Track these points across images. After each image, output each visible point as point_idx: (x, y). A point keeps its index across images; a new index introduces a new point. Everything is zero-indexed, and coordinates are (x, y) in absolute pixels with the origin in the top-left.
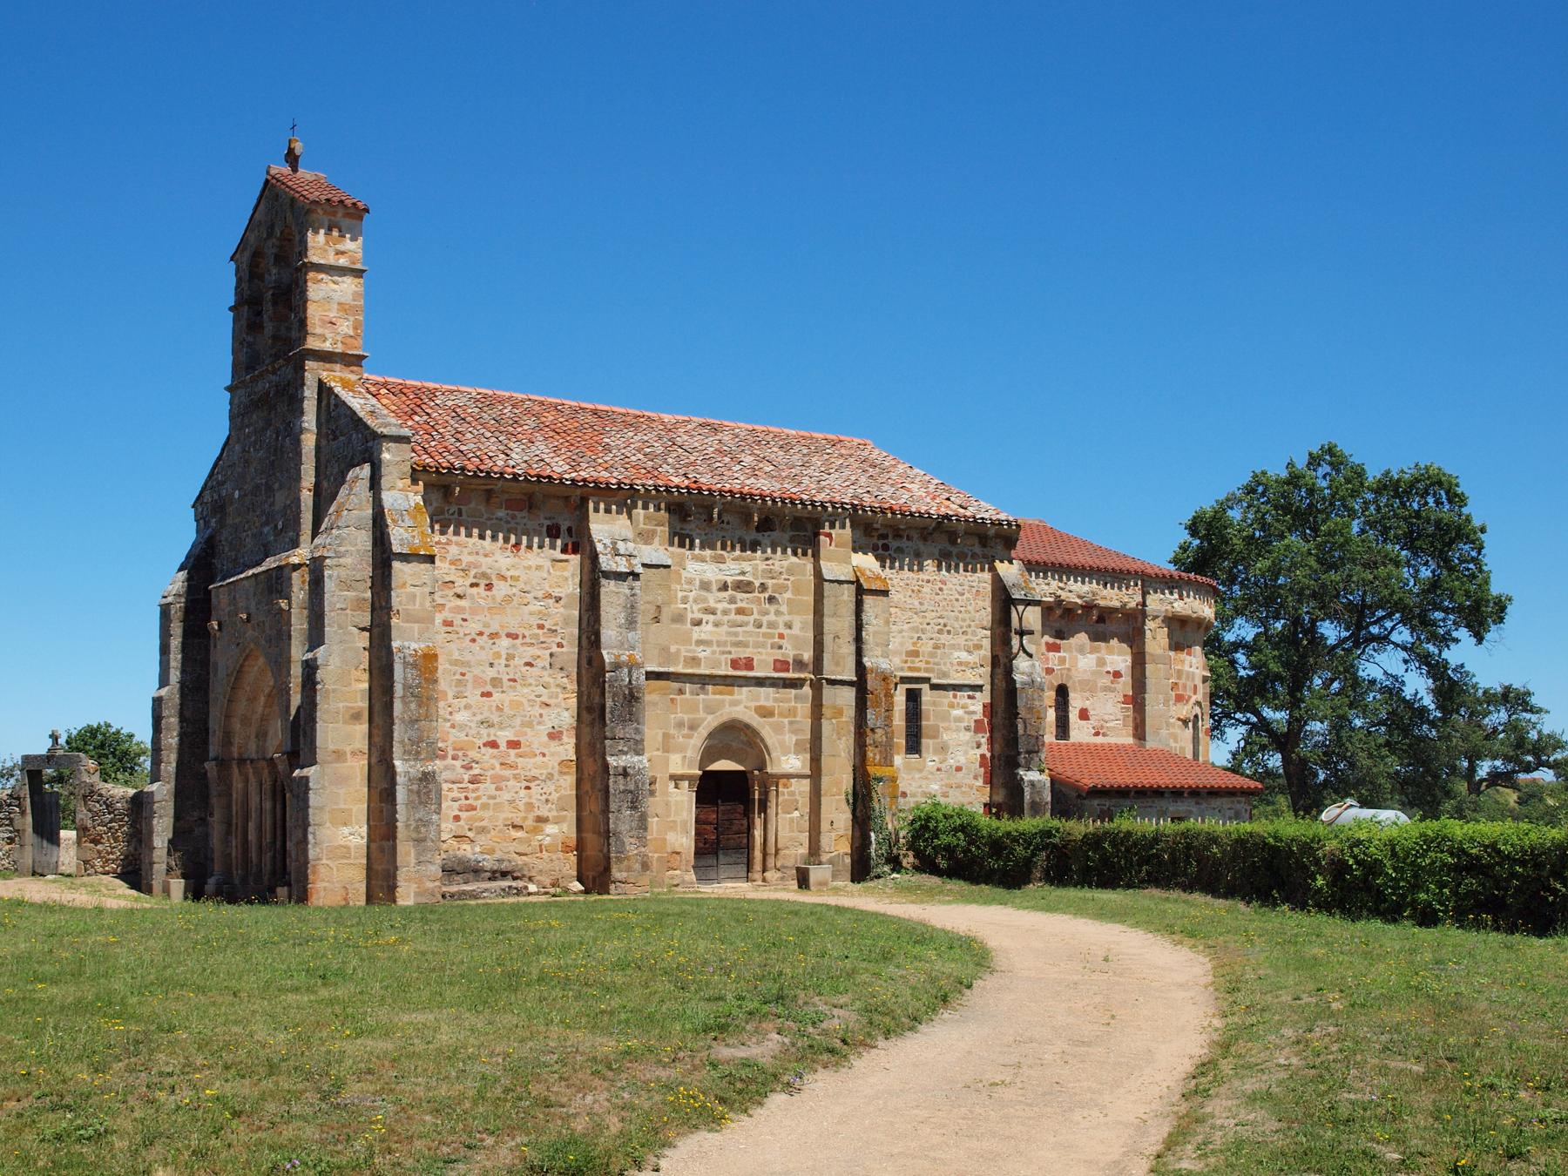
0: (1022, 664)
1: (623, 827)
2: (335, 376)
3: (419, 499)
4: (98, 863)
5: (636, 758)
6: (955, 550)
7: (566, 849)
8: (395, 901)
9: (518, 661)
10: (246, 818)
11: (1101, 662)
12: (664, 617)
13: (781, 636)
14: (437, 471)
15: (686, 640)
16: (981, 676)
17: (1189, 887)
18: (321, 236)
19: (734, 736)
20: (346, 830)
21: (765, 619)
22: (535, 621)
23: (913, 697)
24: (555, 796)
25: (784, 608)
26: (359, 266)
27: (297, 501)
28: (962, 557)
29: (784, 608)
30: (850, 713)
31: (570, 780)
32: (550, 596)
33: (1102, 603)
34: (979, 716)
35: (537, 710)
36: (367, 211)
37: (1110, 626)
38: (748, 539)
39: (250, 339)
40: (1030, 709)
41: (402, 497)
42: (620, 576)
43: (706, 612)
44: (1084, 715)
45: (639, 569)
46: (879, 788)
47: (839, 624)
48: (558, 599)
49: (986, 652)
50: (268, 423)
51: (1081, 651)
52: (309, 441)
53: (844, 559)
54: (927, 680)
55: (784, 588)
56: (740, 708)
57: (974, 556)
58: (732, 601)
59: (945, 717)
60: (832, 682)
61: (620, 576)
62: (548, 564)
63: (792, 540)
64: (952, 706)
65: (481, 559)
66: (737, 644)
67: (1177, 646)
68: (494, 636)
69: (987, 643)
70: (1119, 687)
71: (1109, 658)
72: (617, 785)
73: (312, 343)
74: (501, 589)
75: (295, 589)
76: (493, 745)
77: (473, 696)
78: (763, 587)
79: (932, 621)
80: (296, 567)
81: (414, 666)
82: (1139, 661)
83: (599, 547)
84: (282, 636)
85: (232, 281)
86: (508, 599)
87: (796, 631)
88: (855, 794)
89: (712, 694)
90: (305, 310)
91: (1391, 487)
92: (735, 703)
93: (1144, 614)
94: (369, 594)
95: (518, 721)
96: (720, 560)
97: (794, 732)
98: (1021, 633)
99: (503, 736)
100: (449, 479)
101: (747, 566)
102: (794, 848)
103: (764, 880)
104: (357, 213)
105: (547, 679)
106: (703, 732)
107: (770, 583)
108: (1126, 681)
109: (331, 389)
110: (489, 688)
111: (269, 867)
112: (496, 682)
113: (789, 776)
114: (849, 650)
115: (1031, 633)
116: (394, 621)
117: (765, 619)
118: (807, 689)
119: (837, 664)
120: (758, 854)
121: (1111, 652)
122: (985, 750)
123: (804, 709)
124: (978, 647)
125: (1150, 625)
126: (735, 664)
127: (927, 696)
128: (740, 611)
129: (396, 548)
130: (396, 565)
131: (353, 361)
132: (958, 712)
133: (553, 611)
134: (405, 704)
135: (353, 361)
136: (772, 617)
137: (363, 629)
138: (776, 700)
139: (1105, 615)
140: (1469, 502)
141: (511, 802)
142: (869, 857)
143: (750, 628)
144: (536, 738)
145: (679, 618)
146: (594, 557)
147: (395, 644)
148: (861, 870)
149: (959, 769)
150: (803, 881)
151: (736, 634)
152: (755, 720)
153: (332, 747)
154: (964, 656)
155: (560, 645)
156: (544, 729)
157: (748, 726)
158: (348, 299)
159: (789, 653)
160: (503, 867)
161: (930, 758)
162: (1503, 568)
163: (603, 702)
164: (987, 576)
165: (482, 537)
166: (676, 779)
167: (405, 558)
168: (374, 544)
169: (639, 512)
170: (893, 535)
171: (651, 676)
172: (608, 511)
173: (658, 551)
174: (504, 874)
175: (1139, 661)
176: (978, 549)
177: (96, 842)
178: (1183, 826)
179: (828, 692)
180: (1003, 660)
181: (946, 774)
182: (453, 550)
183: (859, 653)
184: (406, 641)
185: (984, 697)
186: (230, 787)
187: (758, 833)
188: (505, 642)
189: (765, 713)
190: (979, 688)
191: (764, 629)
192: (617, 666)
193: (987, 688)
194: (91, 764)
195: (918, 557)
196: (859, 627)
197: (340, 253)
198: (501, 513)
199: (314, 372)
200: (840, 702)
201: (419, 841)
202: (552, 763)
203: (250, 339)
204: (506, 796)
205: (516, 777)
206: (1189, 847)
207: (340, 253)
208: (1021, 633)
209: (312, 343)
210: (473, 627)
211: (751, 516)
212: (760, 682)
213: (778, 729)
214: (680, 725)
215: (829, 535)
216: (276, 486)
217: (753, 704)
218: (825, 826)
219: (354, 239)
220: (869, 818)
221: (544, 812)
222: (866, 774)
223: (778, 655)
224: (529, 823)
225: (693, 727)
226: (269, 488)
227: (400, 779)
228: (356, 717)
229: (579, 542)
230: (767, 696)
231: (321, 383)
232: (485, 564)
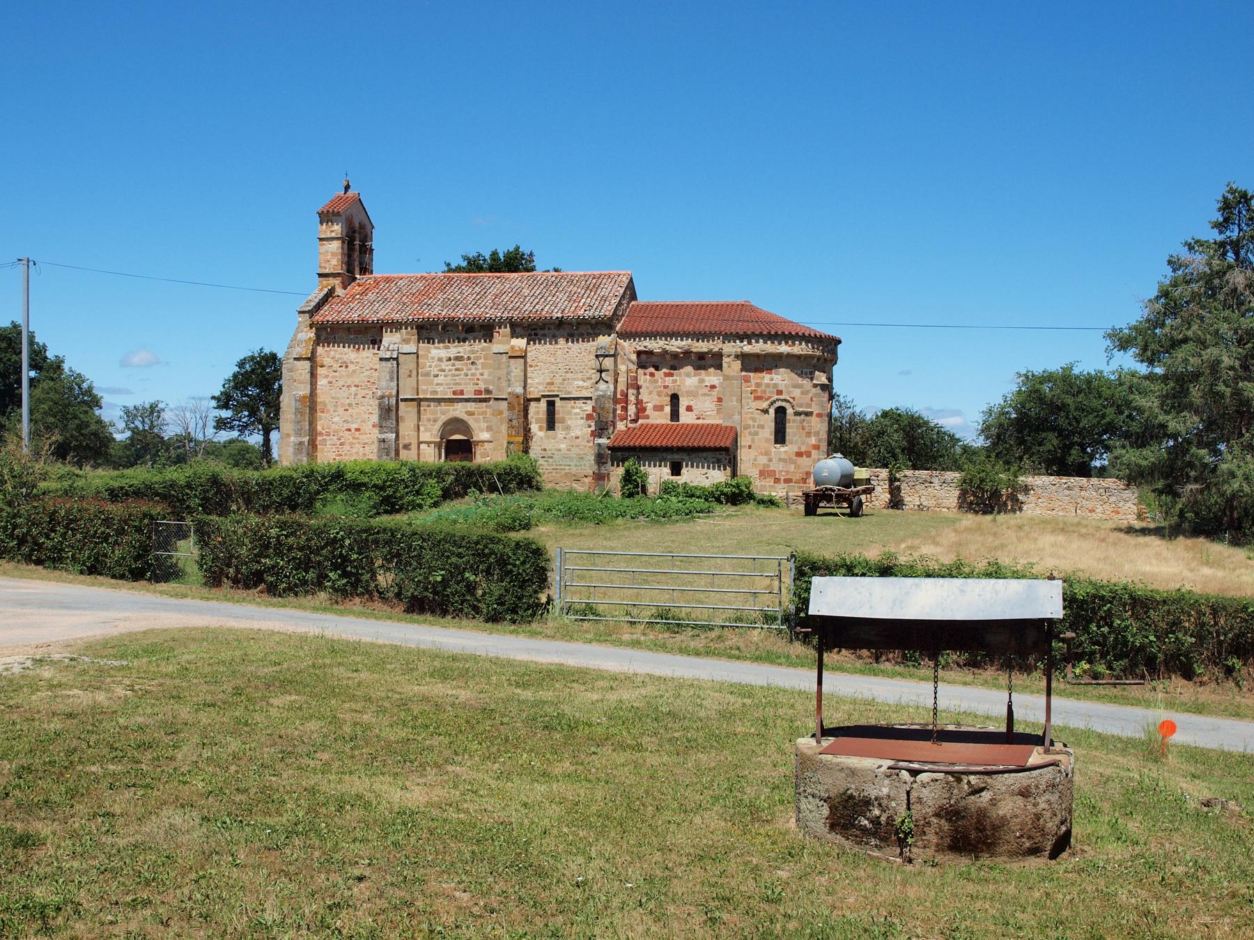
3: (312, 335)
11: (701, 381)
15: (431, 383)
19: (456, 424)
23: (551, 404)
28: (581, 335)
44: (689, 409)
51: (688, 375)
53: (505, 342)
57: (589, 334)
59: (569, 413)
71: (707, 378)
74: (352, 367)
77: (341, 411)
78: (469, 358)
79: (563, 367)
86: (354, 371)
87: (485, 376)
89: (444, 407)
96: (448, 348)
99: (353, 427)
101: (460, 349)
106: (440, 423)
112: (350, 405)
125: (725, 360)
127: (558, 403)
128: (457, 370)
139: (701, 356)
145: (427, 374)
152: (465, 417)
154: (581, 383)
158: (335, 250)
161: (559, 432)
166: (428, 443)
170: (537, 330)
182: (332, 353)
188: (354, 389)
189: (470, 414)
204: (355, 450)
210: (341, 383)
213: (477, 421)
214: (429, 420)
223: (477, 388)
225: (435, 421)
230: (471, 406)
232: (345, 358)
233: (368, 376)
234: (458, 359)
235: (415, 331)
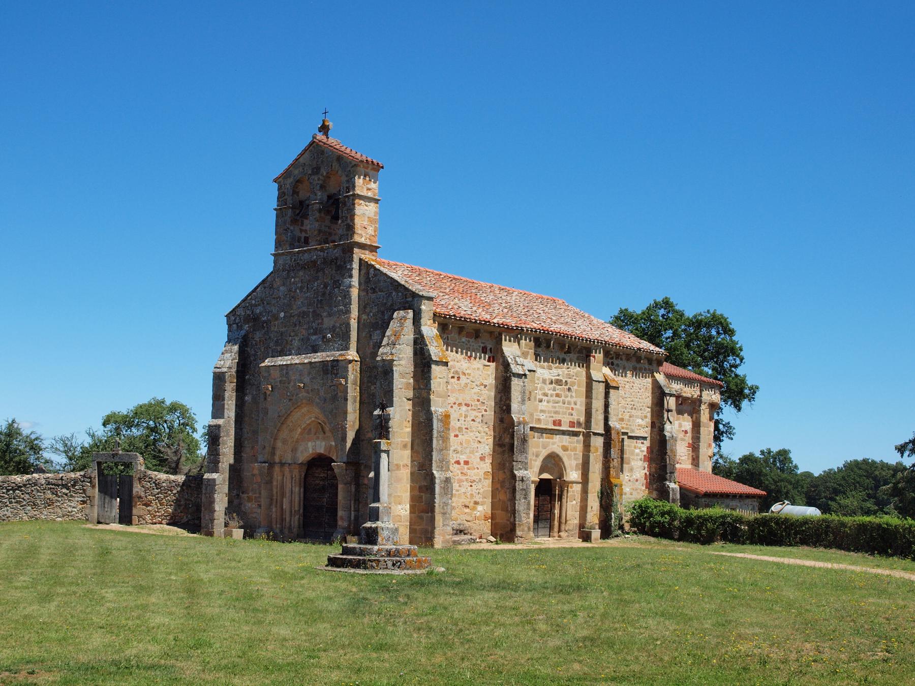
0: (668, 427)
1: (521, 508)
2: (367, 256)
4: (148, 517)
5: (526, 472)
6: (638, 366)
7: (486, 519)
8: (432, 545)
9: (469, 419)
10: (283, 495)
11: (680, 426)
12: (532, 398)
13: (572, 409)
14: (445, 317)
15: (536, 410)
16: (646, 432)
17: (828, 546)
18: (361, 181)
20: (400, 507)
21: (567, 400)
22: (476, 398)
24: (481, 491)
25: (574, 394)
26: (377, 197)
27: (348, 326)
28: (640, 369)
29: (574, 394)
30: (601, 450)
31: (488, 483)
32: (482, 384)
33: (684, 395)
34: (645, 453)
35: (476, 445)
36: (382, 167)
37: (685, 407)
38: (561, 357)
39: (292, 228)
40: (672, 450)
41: (430, 330)
42: (520, 376)
43: (549, 395)
45: (527, 373)
46: (616, 490)
47: (598, 404)
48: (485, 386)
49: (649, 420)
50: (317, 279)
52: (355, 292)
53: (600, 371)
54: (626, 434)
55: (573, 384)
56: (555, 446)
57: (645, 369)
58: (554, 390)
59: (632, 453)
60: (595, 434)
61: (520, 376)
62: (482, 367)
63: (578, 359)
64: (635, 447)
65: (456, 363)
66: (556, 413)
67: (680, 412)
68: (460, 404)
69: (649, 415)
70: (686, 438)
71: (683, 423)
72: (519, 486)
73: (357, 238)
75: (350, 373)
76: (458, 462)
80: (350, 362)
81: (441, 421)
82: (696, 426)
83: (510, 361)
84: (338, 397)
85: (276, 193)
87: (578, 406)
88: (602, 493)
90: (353, 220)
91: (697, 324)
92: (553, 444)
93: (700, 402)
94: (412, 381)
95: (468, 451)
97: (575, 459)
98: (668, 411)
99: (463, 458)
100: (446, 321)
101: (560, 371)
102: (573, 519)
103: (559, 536)
104: (378, 167)
105: (480, 429)
106: (541, 458)
107: (569, 380)
108: (689, 435)
109: (373, 266)
110: (457, 433)
111: (296, 523)
113: (573, 482)
114: (601, 417)
115: (671, 411)
116: (432, 397)
117: (567, 400)
118: (581, 437)
119: (597, 424)
120: (556, 523)
121: (684, 421)
122: (646, 471)
123: (580, 447)
124: (646, 417)
125: (703, 407)
126: (555, 423)
127: (627, 442)
128: (557, 395)
129: (434, 358)
130: (433, 366)
131: (373, 249)
132: (637, 451)
133: (483, 392)
134: (438, 441)
135: (373, 249)
136: (569, 399)
137: (409, 400)
138: (570, 442)
140: (737, 333)
141: (465, 493)
142: (610, 525)
143: (561, 404)
144: (475, 460)
146: (506, 365)
147: (433, 409)
148: (606, 533)
149: (637, 480)
150: (586, 536)
151: (555, 407)
153: (395, 462)
155: (486, 411)
156: (478, 455)
157: (558, 456)
158: (372, 215)
159: (575, 418)
160: (461, 527)
162: (748, 370)
163: (507, 440)
164: (650, 380)
165: (457, 352)
167: (437, 363)
168: (415, 354)
169: (523, 342)
171: (532, 429)
172: (510, 341)
173: (530, 363)
174: (461, 531)
175: (696, 426)
176: (647, 366)
177: (147, 505)
178: (734, 513)
179: (593, 438)
180: (657, 425)
181: (633, 485)
183: (606, 419)
184: (437, 407)
185: (647, 443)
186: (272, 478)
187: (557, 512)
188: (464, 408)
189: (565, 449)
190: (645, 438)
191: (566, 405)
192: (519, 423)
193: (649, 439)
194: (141, 459)
195: (625, 369)
196: (607, 406)
197: (369, 189)
198: (463, 340)
199: (358, 254)
200: (597, 444)
201: (444, 514)
202: (481, 472)
203: (292, 228)
204: (463, 490)
205: (467, 480)
206: (828, 527)
207: (369, 189)
208: (668, 411)
209: (357, 238)
211: (565, 345)
212: (563, 433)
213: (569, 457)
215: (594, 357)
216: (325, 314)
217: (560, 444)
218: (589, 509)
219: (375, 182)
220: (611, 506)
221: (477, 500)
222: (610, 483)
223: (571, 419)
224: (471, 505)
225: (537, 456)
226: (317, 315)
227: (437, 481)
228: (405, 446)
229: (495, 355)
231: (360, 260)
233: (480, 395)
234: (559, 382)
235: (532, 343)
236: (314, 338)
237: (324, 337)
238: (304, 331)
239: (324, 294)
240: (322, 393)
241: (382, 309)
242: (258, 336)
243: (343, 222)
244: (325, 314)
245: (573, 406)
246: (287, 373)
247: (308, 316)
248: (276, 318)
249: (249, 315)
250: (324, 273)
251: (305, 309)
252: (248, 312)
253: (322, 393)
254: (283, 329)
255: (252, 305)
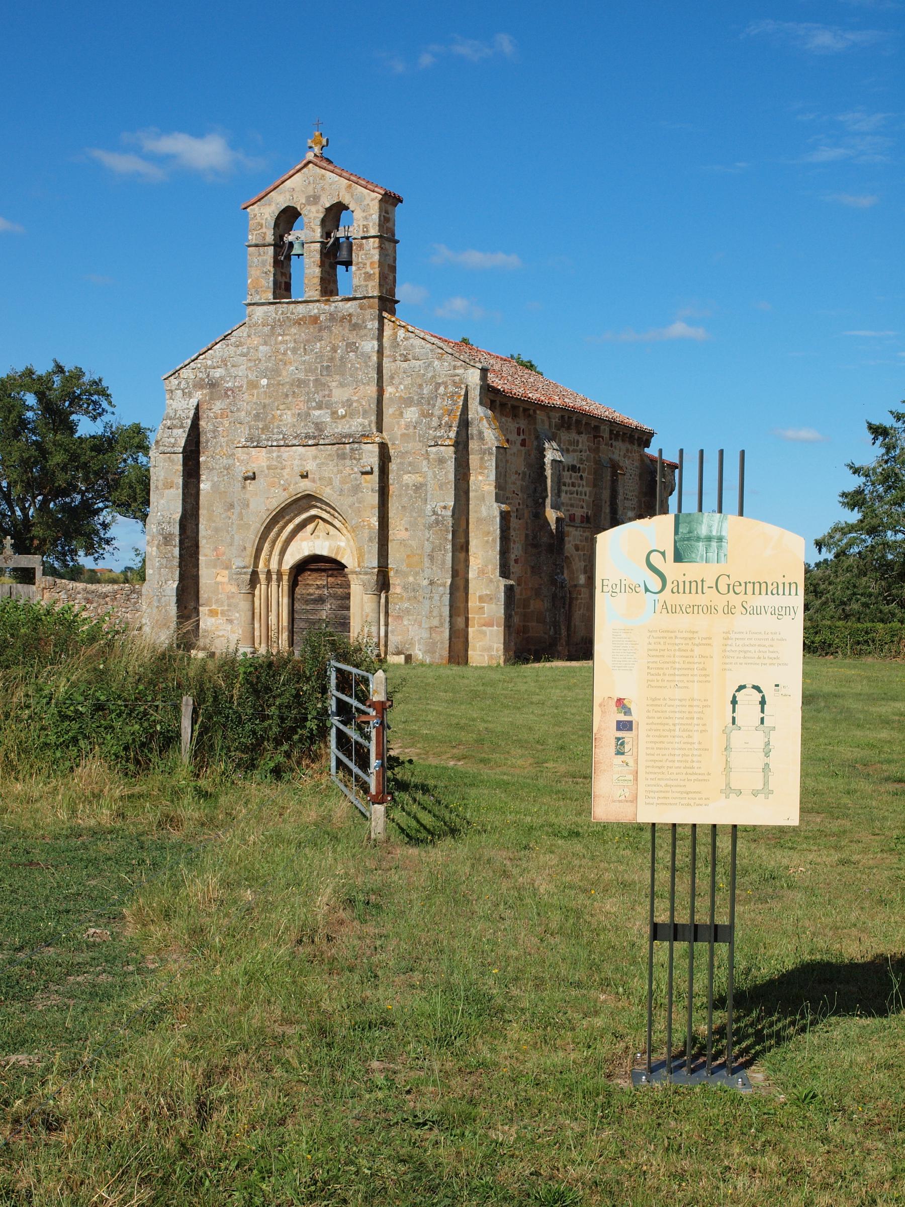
21: (580, 489)
36: (401, 202)
66: (572, 505)
107: (581, 466)
143: (575, 495)
234: (573, 468)
236: (317, 413)
237: (336, 413)
238: (301, 405)
239: (332, 359)
240: (336, 482)
241: (419, 381)
242: (218, 406)
243: (359, 269)
244: (334, 384)
245: (583, 497)
246: (278, 457)
247: (308, 384)
248: (253, 385)
249: (202, 379)
250: (331, 331)
251: (302, 376)
252: (201, 375)
253: (336, 482)
254: (267, 401)
255: (206, 367)
